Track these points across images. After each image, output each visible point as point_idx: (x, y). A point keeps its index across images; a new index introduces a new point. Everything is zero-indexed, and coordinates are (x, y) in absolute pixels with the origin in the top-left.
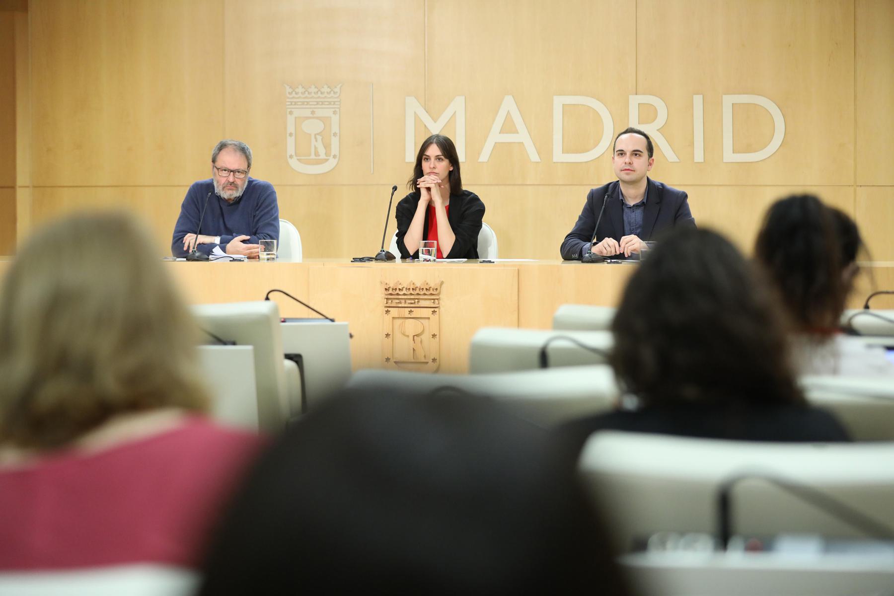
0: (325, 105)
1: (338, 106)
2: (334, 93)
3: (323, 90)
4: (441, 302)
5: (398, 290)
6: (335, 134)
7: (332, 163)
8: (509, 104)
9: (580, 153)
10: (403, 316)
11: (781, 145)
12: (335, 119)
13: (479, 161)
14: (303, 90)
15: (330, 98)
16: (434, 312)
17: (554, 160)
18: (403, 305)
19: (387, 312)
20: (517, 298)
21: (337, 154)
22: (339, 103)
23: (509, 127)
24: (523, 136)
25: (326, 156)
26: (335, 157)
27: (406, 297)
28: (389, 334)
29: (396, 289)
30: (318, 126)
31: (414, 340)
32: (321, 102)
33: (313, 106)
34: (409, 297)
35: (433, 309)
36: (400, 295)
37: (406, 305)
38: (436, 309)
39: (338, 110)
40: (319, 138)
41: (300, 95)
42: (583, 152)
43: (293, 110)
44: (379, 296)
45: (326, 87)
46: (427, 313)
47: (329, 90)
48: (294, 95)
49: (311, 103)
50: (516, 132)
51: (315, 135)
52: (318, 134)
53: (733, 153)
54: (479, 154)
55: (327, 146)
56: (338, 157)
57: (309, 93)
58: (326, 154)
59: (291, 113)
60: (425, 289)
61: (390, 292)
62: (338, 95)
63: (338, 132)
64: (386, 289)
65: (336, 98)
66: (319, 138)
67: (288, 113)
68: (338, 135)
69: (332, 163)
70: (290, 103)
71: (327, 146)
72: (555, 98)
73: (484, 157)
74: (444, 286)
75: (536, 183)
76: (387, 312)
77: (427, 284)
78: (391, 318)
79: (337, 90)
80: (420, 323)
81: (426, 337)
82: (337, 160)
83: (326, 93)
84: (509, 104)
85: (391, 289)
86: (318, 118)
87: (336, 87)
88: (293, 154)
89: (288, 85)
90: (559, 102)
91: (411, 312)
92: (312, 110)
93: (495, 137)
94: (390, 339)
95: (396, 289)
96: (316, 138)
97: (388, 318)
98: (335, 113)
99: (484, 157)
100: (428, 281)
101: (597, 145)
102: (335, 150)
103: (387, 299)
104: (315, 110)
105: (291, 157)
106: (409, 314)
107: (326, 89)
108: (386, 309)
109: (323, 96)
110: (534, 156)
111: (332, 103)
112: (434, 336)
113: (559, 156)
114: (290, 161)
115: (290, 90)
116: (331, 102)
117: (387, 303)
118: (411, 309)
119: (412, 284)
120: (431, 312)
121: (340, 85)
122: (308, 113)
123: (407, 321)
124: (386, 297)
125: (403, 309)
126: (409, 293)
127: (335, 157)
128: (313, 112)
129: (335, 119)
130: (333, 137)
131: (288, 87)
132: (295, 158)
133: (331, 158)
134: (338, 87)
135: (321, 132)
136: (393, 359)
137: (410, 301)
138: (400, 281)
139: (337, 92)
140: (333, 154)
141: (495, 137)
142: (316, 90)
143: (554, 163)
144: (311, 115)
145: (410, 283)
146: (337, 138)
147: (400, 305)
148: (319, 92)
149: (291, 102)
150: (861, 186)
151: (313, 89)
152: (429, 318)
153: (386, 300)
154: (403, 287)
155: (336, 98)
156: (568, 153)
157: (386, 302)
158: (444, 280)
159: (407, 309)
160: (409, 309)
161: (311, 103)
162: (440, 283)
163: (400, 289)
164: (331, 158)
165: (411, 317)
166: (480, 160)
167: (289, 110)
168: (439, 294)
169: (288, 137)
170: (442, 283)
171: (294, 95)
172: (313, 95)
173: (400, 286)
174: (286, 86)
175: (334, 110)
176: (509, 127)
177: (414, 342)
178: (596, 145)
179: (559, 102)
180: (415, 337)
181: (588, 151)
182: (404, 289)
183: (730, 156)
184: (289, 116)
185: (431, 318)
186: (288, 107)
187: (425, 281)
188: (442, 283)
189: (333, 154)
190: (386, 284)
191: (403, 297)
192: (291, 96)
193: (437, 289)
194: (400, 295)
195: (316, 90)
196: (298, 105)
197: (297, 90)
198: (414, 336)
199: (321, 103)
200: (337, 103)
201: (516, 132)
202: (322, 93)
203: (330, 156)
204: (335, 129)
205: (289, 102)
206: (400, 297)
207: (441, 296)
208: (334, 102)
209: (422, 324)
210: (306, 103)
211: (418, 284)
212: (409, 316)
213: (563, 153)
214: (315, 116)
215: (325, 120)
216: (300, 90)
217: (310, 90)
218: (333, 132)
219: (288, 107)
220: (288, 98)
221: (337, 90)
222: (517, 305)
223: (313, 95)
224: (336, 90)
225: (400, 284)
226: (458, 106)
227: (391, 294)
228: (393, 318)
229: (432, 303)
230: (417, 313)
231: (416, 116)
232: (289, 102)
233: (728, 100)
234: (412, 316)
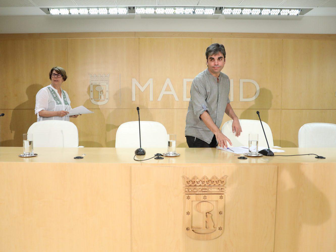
7: (106, 101)
8: (168, 81)
11: (258, 96)
13: (158, 100)
18: (199, 193)
19: (188, 198)
23: (168, 89)
24: (173, 92)
25: (104, 99)
26: (107, 99)
31: (207, 216)
35: (220, 195)
37: (201, 193)
38: (222, 195)
44: (181, 186)
46: (217, 197)
47: (105, 76)
50: (171, 91)
51: (100, 91)
52: (101, 91)
53: (243, 98)
54: (158, 98)
61: (191, 183)
69: (106, 101)
72: (184, 80)
73: (159, 99)
77: (216, 178)
84: (168, 81)
88: (92, 98)
90: (185, 81)
93: (163, 92)
94: (190, 216)
96: (100, 92)
99: (159, 99)
102: (107, 97)
105: (92, 99)
108: (188, 196)
110: (177, 99)
112: (220, 213)
114: (91, 100)
118: (205, 195)
119: (206, 178)
123: (202, 203)
125: (199, 195)
127: (107, 99)
132: (93, 99)
133: (106, 100)
136: (192, 227)
140: (107, 98)
141: (163, 92)
147: (197, 193)
150: (283, 109)
152: (218, 201)
159: (202, 195)
160: (204, 195)
162: (226, 177)
164: (106, 100)
165: (205, 200)
166: (158, 100)
169: (91, 92)
173: (198, 180)
176: (168, 89)
177: (207, 217)
179: (185, 81)
180: (207, 214)
182: (201, 182)
183: (242, 99)
185: (219, 201)
189: (107, 98)
198: (206, 213)
201: (171, 91)
211: (210, 178)
212: (204, 200)
224: (107, 76)
225: (197, 179)
226: (150, 82)
227: (190, 186)
228: (192, 201)
229: (218, 190)
230: (209, 197)
231: (136, 85)
233: (242, 81)
234: (206, 200)
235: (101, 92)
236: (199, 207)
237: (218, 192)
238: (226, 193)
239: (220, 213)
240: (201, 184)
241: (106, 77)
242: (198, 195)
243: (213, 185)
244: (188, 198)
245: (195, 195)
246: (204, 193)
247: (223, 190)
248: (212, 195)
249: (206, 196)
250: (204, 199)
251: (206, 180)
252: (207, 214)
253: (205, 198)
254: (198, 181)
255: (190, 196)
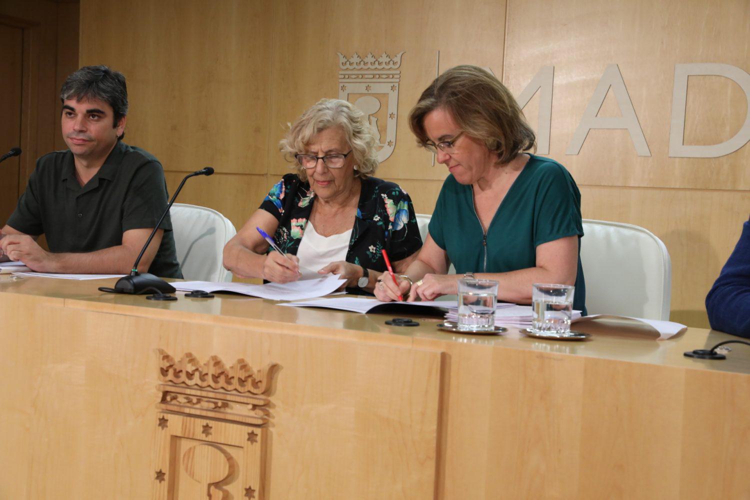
0: (382, 78)
1: (398, 80)
2: (394, 63)
3: (380, 60)
4: (271, 411)
5: (183, 377)
6: (391, 116)
7: (387, 151)
9: (710, 144)
10: (191, 437)
12: (393, 96)
14: (358, 60)
15: (389, 69)
16: (252, 437)
17: (671, 154)
18: (193, 412)
20: (434, 427)
21: (393, 140)
22: (398, 76)
26: (390, 143)
27: (199, 393)
28: (163, 472)
29: (181, 371)
30: (374, 105)
31: (209, 495)
32: (379, 75)
33: (368, 80)
34: (204, 394)
35: (250, 429)
36: (188, 387)
37: (198, 412)
38: (258, 431)
39: (397, 85)
40: (374, 119)
41: (355, 66)
42: (714, 144)
43: (345, 85)
44: (154, 384)
45: (384, 55)
46: (235, 434)
48: (348, 65)
49: (366, 76)
52: (372, 115)
55: (382, 130)
56: (394, 144)
57: (365, 64)
58: (380, 140)
59: (343, 88)
60: (235, 382)
62: (398, 66)
63: (395, 112)
64: (164, 372)
65: (396, 69)
66: (374, 119)
67: (340, 88)
68: (396, 116)
69: (387, 151)
70: (343, 77)
71: (382, 130)
74: (280, 377)
75: (642, 185)
76: (163, 422)
78: (169, 438)
79: (397, 59)
80: (222, 455)
81: (236, 489)
82: (393, 147)
83: (384, 64)
85: (171, 371)
86: (373, 95)
87: (396, 56)
89: (342, 55)
91: (206, 429)
92: (367, 85)
95: (181, 371)
97: (163, 436)
98: (393, 88)
100: (249, 361)
101: (736, 133)
102: (390, 136)
103: (166, 393)
104: (370, 84)
106: (203, 432)
107: (384, 59)
109: (381, 67)
110: (643, 150)
111: (391, 76)
113: (677, 149)
115: (344, 60)
116: (390, 74)
117: (164, 400)
118: (208, 421)
119: (212, 363)
120: (247, 437)
121: (401, 54)
122: (362, 88)
124: (162, 389)
125: (192, 419)
126: (205, 384)
127: (390, 143)
128: (367, 88)
129: (393, 96)
130: (389, 120)
131: (341, 57)
134: (399, 56)
135: (375, 113)
137: (205, 404)
138: (195, 354)
139: (397, 62)
142: (373, 60)
143: (670, 157)
144: (366, 92)
145: (208, 362)
146: (395, 120)
147: (187, 411)
148: (377, 63)
149: (344, 75)
151: (370, 59)
153: (161, 395)
154: (194, 368)
155: (396, 69)
156: (691, 144)
157: (160, 400)
158: (279, 362)
160: (205, 422)
161: (366, 76)
163: (190, 376)
167: (342, 85)
168: (267, 392)
170: (274, 369)
171: (348, 65)
172: (369, 66)
174: (339, 54)
175: (392, 85)
178: (734, 133)
181: (721, 142)
182: (197, 374)
184: (341, 91)
185: (245, 449)
186: (340, 81)
187: (241, 361)
188: (274, 369)
190: (166, 357)
191: (193, 392)
192: (345, 68)
193: (260, 381)
194: (188, 387)
195: (373, 60)
196: (352, 78)
197: (352, 60)
199: (378, 76)
200: (395, 76)
202: (380, 64)
203: (384, 143)
204: (392, 109)
205: (342, 74)
206: (188, 391)
207: (272, 399)
208: (393, 75)
209: (229, 458)
210: (360, 76)
212: (203, 437)
213: (683, 144)
214: (370, 92)
215: (382, 98)
216: (355, 59)
217: (366, 60)
218: (390, 112)
219: (340, 81)
220: (343, 70)
221: (397, 59)
222: (433, 444)
223: (369, 66)
224: (395, 60)
228: (175, 438)
232: (342, 74)
234: (210, 438)
235: (372, 118)
236: (190, 460)
237: (246, 416)
238: (274, 426)
239: (249, 492)
240: (199, 383)
241: (391, 65)
242: (188, 418)
243: (230, 388)
244: (163, 422)
245: (181, 418)
246: (204, 413)
247: (259, 413)
248: (228, 425)
249: (210, 425)
250: (204, 435)
251: (212, 370)
252: (212, 488)
253: (206, 429)
254: (190, 371)
255: (169, 419)
